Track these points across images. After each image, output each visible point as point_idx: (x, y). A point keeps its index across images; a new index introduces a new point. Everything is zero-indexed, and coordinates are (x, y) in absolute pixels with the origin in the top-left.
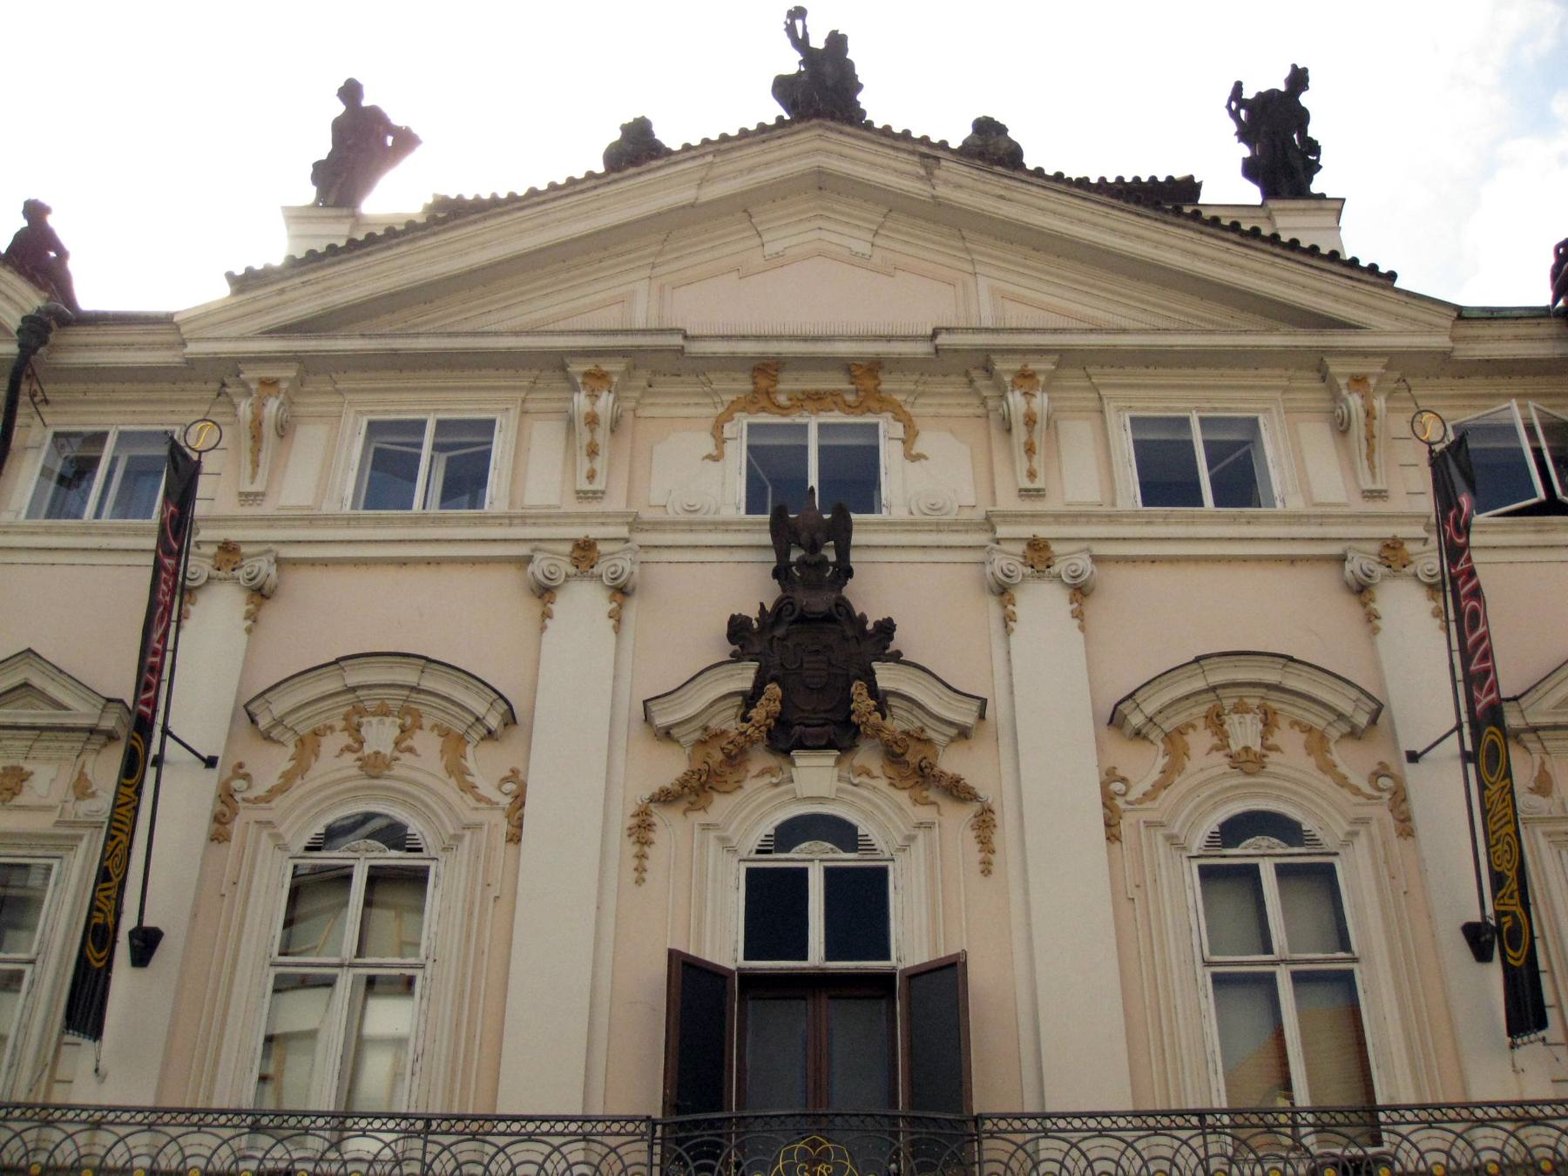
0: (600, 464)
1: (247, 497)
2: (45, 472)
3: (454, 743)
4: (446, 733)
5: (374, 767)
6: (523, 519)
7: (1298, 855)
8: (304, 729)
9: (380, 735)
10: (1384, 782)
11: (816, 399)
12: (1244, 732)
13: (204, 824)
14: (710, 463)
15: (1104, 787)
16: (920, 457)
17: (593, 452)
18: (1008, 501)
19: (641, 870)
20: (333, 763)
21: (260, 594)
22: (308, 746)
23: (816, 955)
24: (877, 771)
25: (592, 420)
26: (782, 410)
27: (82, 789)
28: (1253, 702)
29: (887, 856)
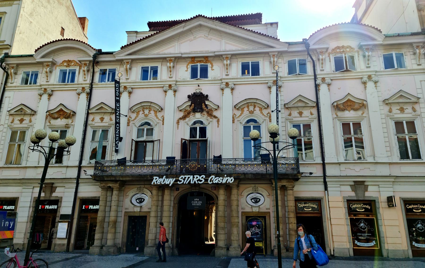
0: (172, 73)
1: (127, 79)
2: (100, 74)
3: (156, 112)
4: (154, 111)
5: (146, 116)
6: (162, 82)
7: (256, 125)
8: (137, 111)
9: (147, 112)
10: (269, 115)
11: (200, 61)
12: (251, 108)
13: (126, 124)
15: (233, 116)
17: (171, 71)
18: (224, 77)
19: (178, 128)
20: (141, 115)
21: (130, 93)
22: (138, 113)
23: (198, 138)
25: (170, 67)
27: (111, 120)
28: (253, 104)
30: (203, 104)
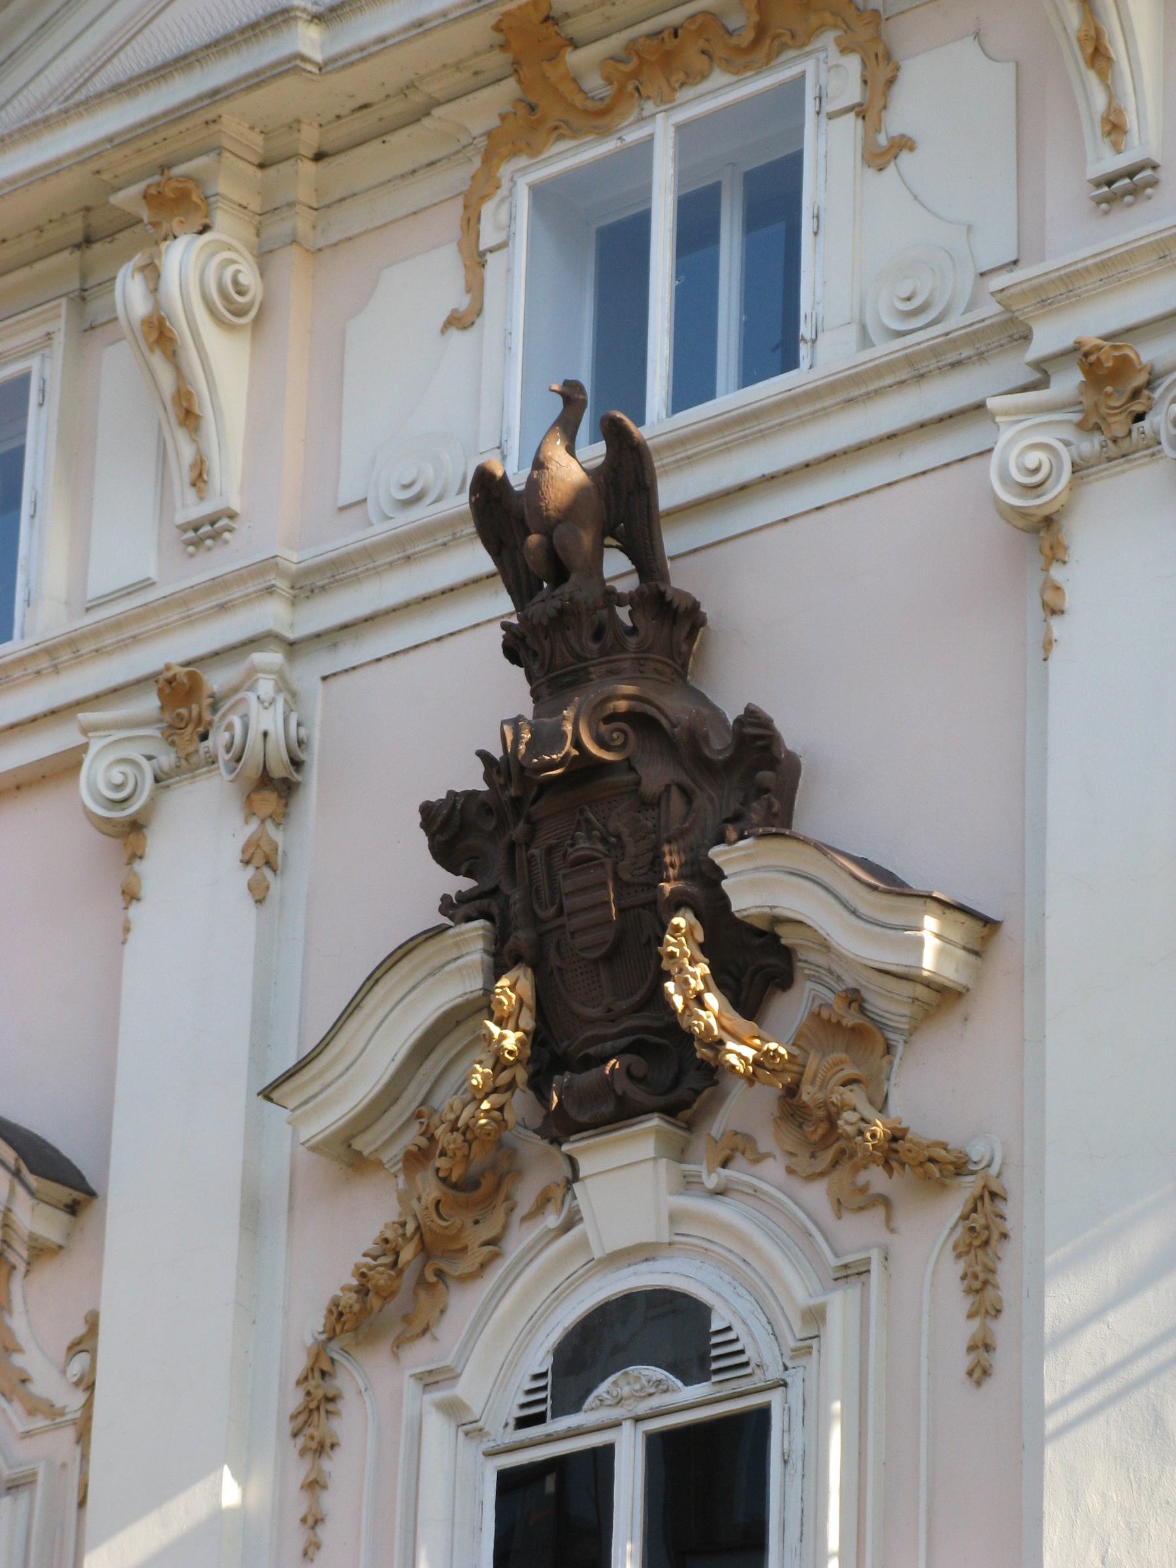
14: (455, 335)
16: (903, 144)
19: (314, 1521)
24: (766, 1142)
26: (599, 117)
29: (774, 1372)
30: (682, 933)
